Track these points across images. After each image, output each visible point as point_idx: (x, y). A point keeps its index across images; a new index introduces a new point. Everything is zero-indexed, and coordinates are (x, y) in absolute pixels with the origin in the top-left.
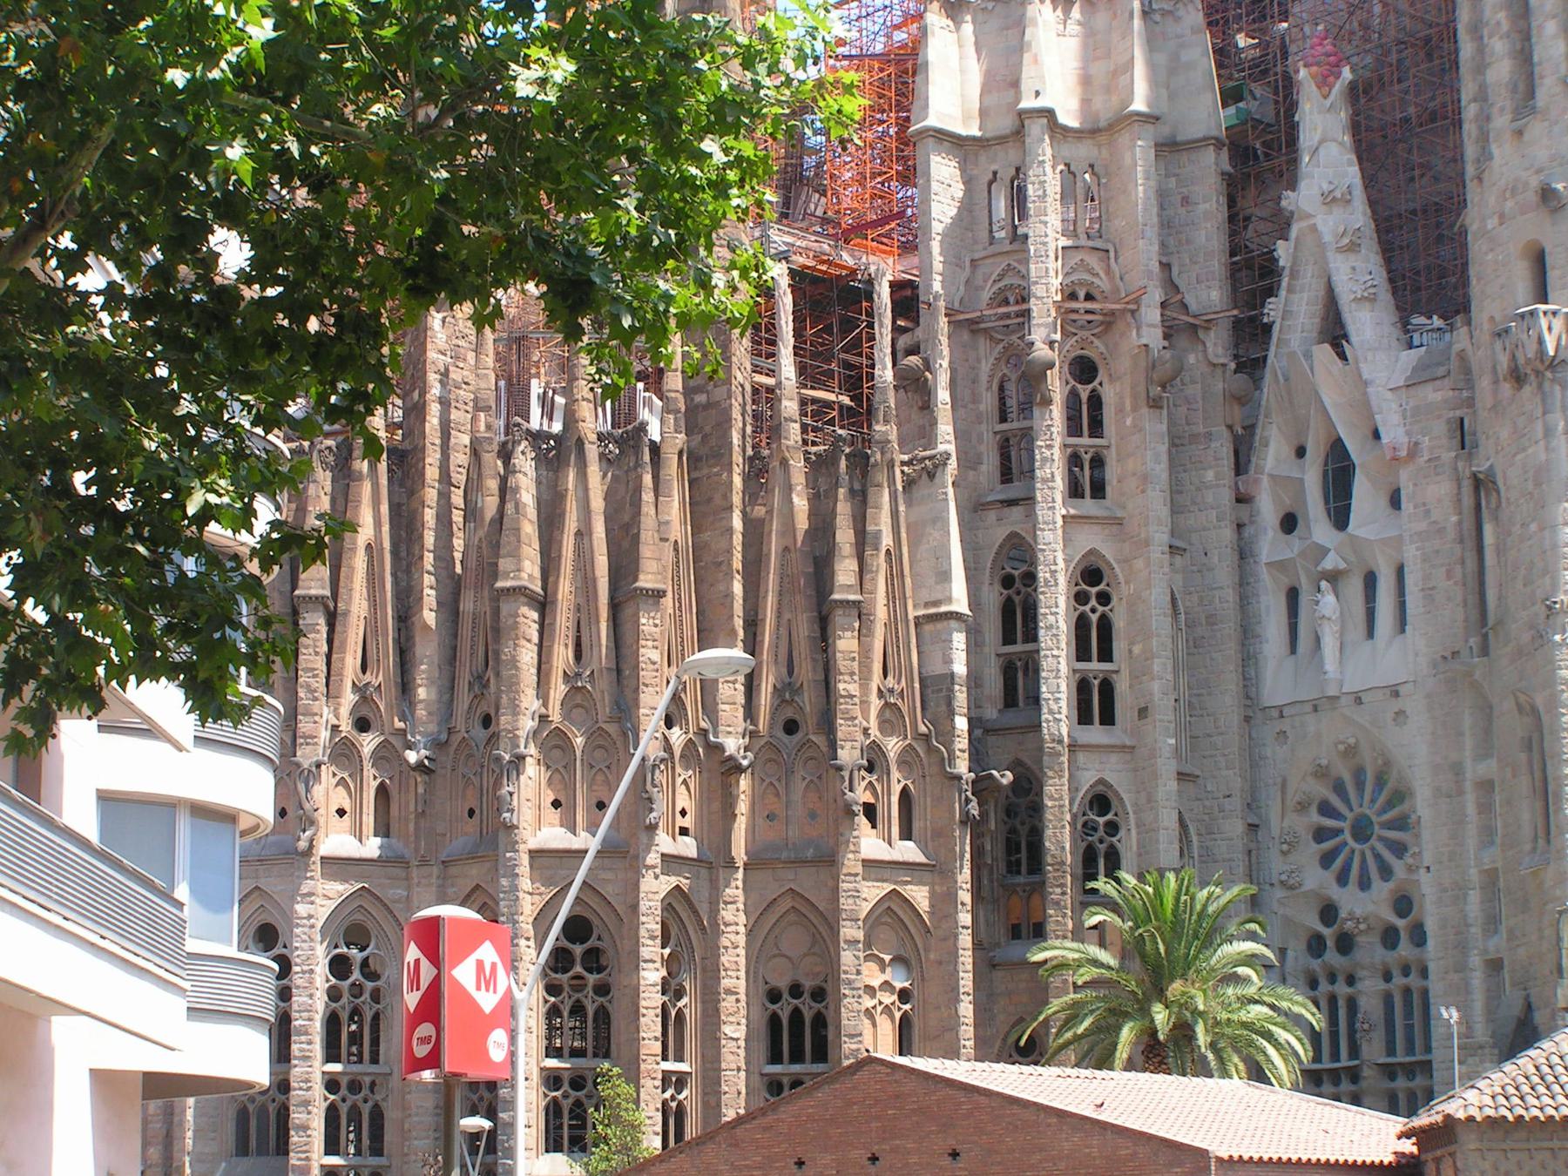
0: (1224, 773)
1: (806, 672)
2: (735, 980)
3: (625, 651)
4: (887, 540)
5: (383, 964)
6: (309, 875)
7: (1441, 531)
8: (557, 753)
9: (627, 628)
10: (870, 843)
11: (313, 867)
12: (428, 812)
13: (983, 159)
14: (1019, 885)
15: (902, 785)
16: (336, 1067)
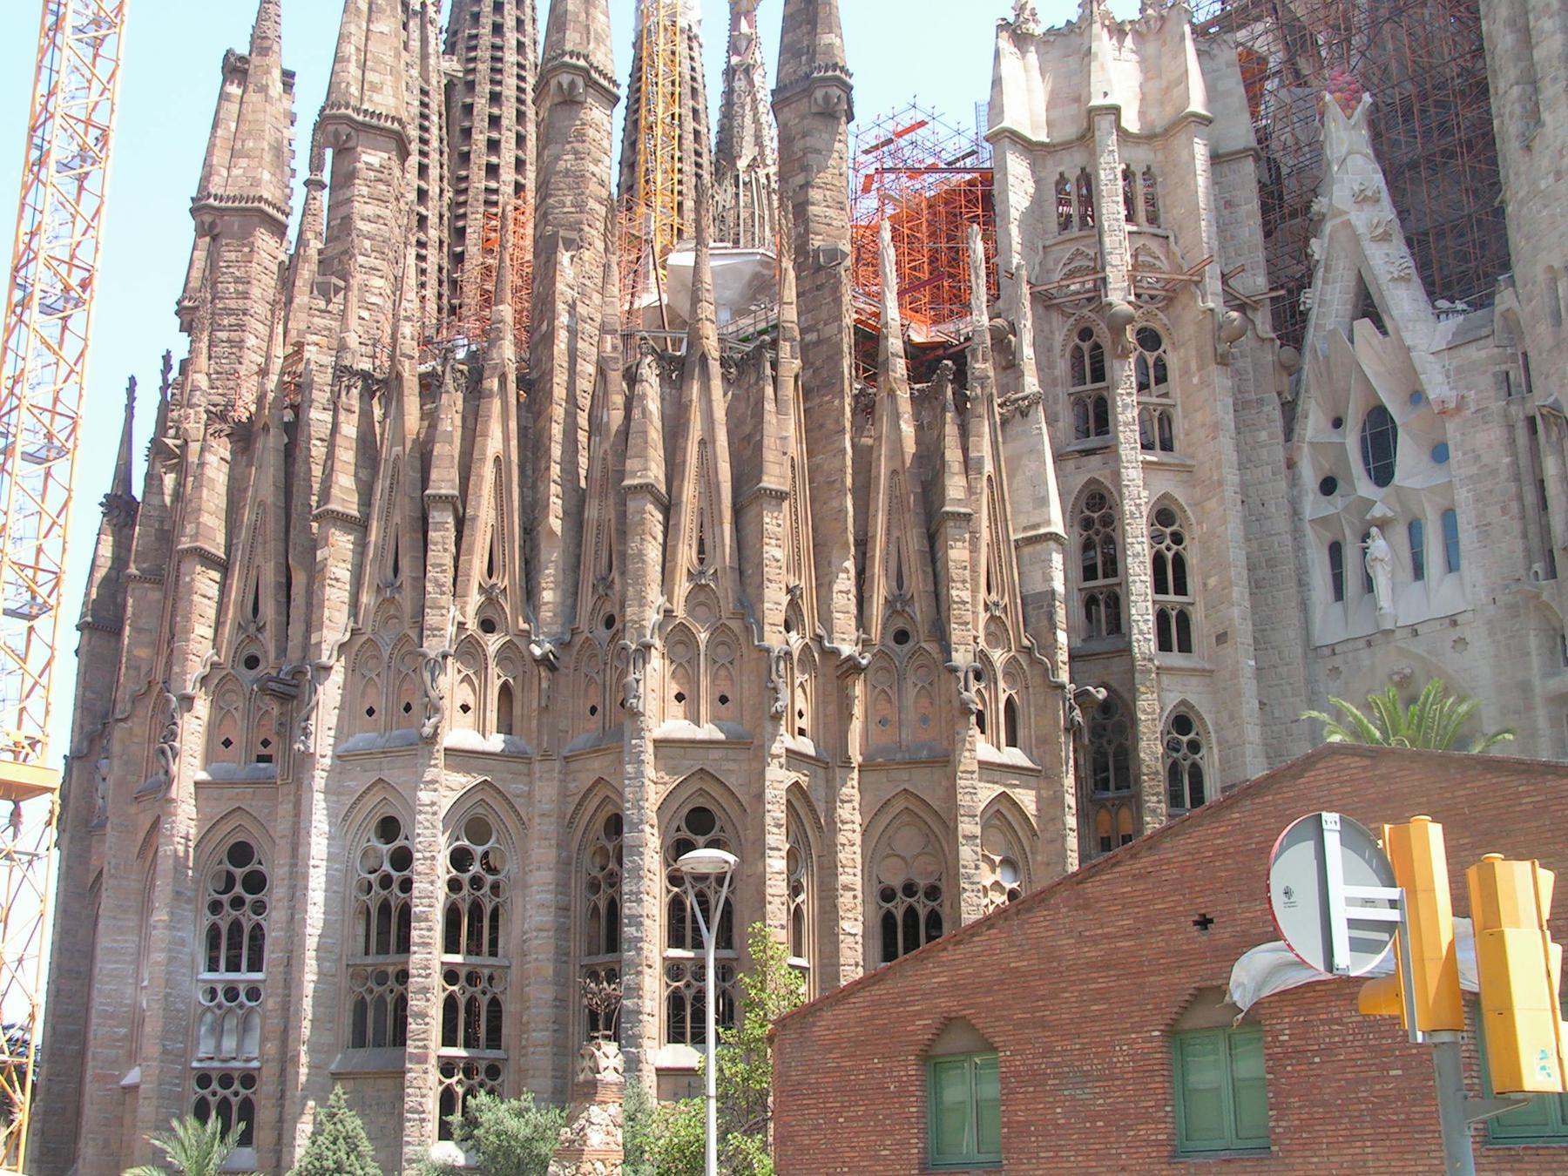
0: (1291, 700)
1: (917, 583)
2: (852, 877)
3: (747, 552)
4: (988, 468)
5: (503, 857)
6: (433, 762)
7: (1493, 473)
8: (680, 648)
9: (750, 531)
10: (983, 748)
11: (436, 755)
12: (551, 708)
13: (1050, 162)
14: (1108, 799)
15: (1007, 694)
16: (457, 958)
